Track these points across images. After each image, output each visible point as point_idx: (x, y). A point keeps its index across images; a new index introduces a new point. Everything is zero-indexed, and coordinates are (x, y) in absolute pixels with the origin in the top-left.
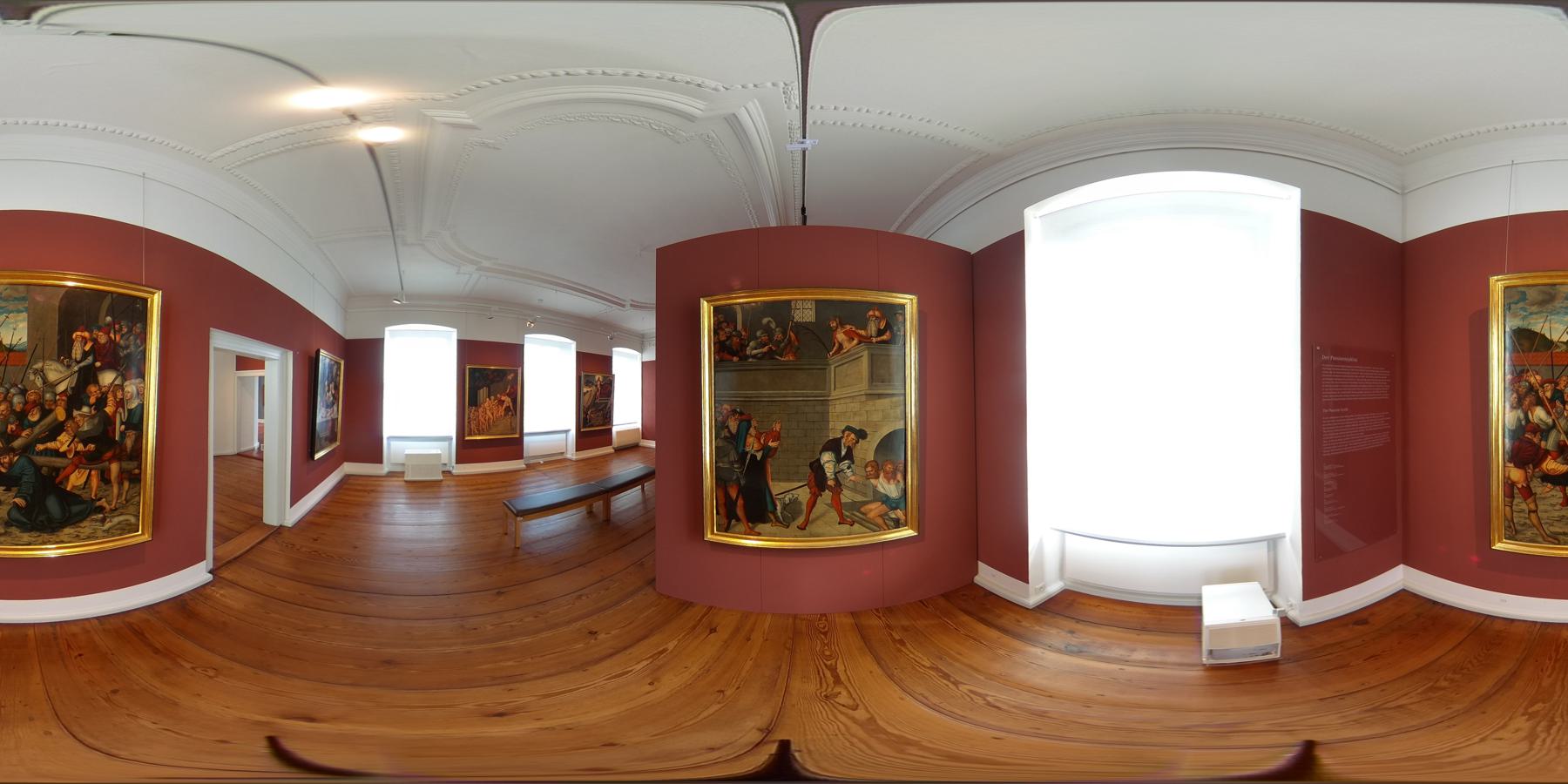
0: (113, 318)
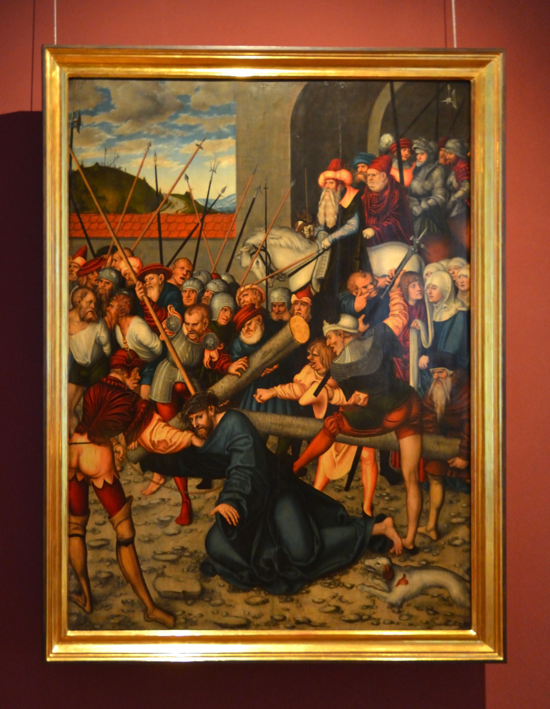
0: (397, 137)
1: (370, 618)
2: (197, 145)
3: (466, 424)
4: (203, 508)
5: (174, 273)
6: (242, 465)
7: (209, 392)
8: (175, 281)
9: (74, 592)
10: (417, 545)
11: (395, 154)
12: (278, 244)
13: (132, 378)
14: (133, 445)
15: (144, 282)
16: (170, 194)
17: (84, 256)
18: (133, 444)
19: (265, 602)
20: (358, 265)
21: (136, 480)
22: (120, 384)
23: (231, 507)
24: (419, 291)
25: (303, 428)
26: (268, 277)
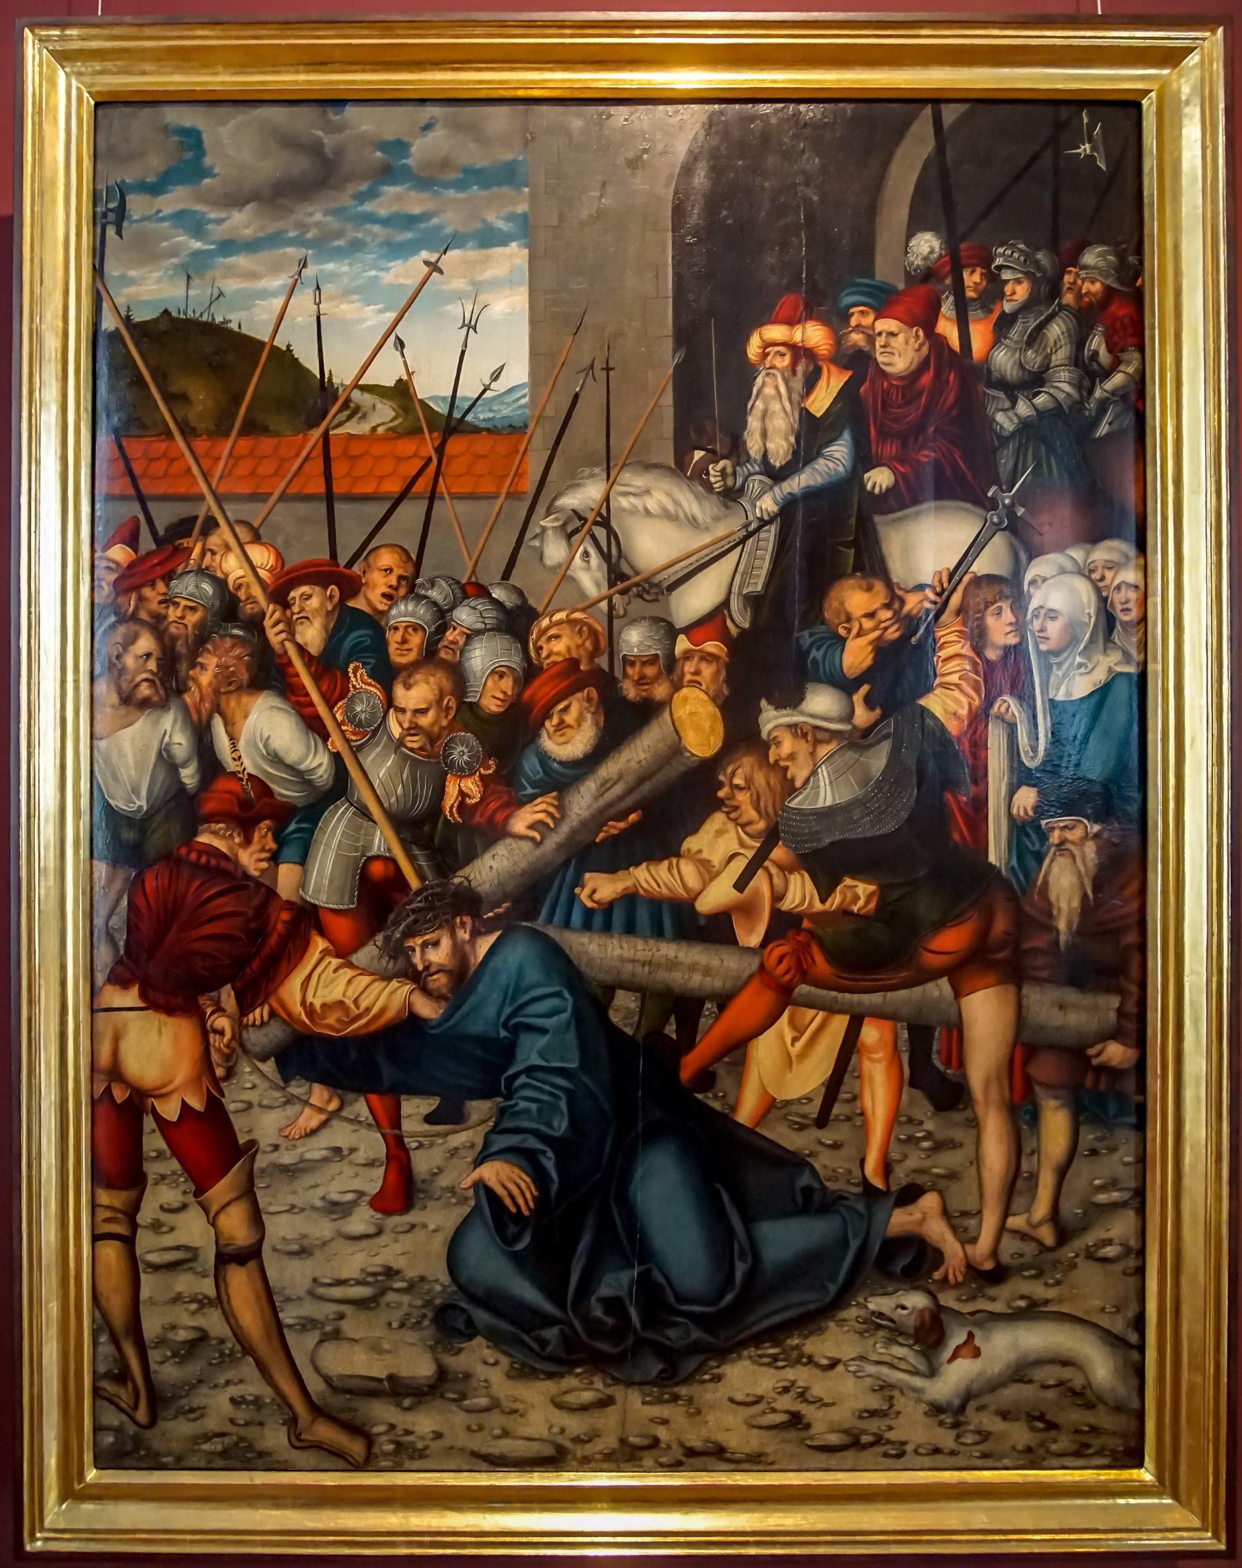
1: (879, 1440)
2: (427, 263)
3: (1136, 959)
4: (441, 1170)
5: (366, 583)
6: (543, 1063)
7: (456, 881)
8: (369, 602)
9: (108, 1375)
10: (1005, 1258)
11: (948, 281)
12: (640, 507)
13: (255, 846)
14: (257, 1015)
15: (286, 605)
16: (356, 385)
17: (132, 540)
18: (258, 1011)
19: (605, 1403)
20: (851, 560)
21: (265, 1102)
22: (223, 864)
23: (516, 1170)
24: (1011, 624)
25: (707, 971)
26: (613, 590)
